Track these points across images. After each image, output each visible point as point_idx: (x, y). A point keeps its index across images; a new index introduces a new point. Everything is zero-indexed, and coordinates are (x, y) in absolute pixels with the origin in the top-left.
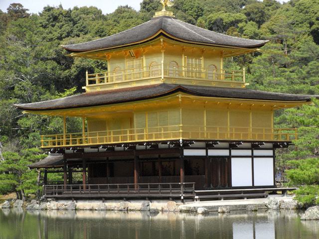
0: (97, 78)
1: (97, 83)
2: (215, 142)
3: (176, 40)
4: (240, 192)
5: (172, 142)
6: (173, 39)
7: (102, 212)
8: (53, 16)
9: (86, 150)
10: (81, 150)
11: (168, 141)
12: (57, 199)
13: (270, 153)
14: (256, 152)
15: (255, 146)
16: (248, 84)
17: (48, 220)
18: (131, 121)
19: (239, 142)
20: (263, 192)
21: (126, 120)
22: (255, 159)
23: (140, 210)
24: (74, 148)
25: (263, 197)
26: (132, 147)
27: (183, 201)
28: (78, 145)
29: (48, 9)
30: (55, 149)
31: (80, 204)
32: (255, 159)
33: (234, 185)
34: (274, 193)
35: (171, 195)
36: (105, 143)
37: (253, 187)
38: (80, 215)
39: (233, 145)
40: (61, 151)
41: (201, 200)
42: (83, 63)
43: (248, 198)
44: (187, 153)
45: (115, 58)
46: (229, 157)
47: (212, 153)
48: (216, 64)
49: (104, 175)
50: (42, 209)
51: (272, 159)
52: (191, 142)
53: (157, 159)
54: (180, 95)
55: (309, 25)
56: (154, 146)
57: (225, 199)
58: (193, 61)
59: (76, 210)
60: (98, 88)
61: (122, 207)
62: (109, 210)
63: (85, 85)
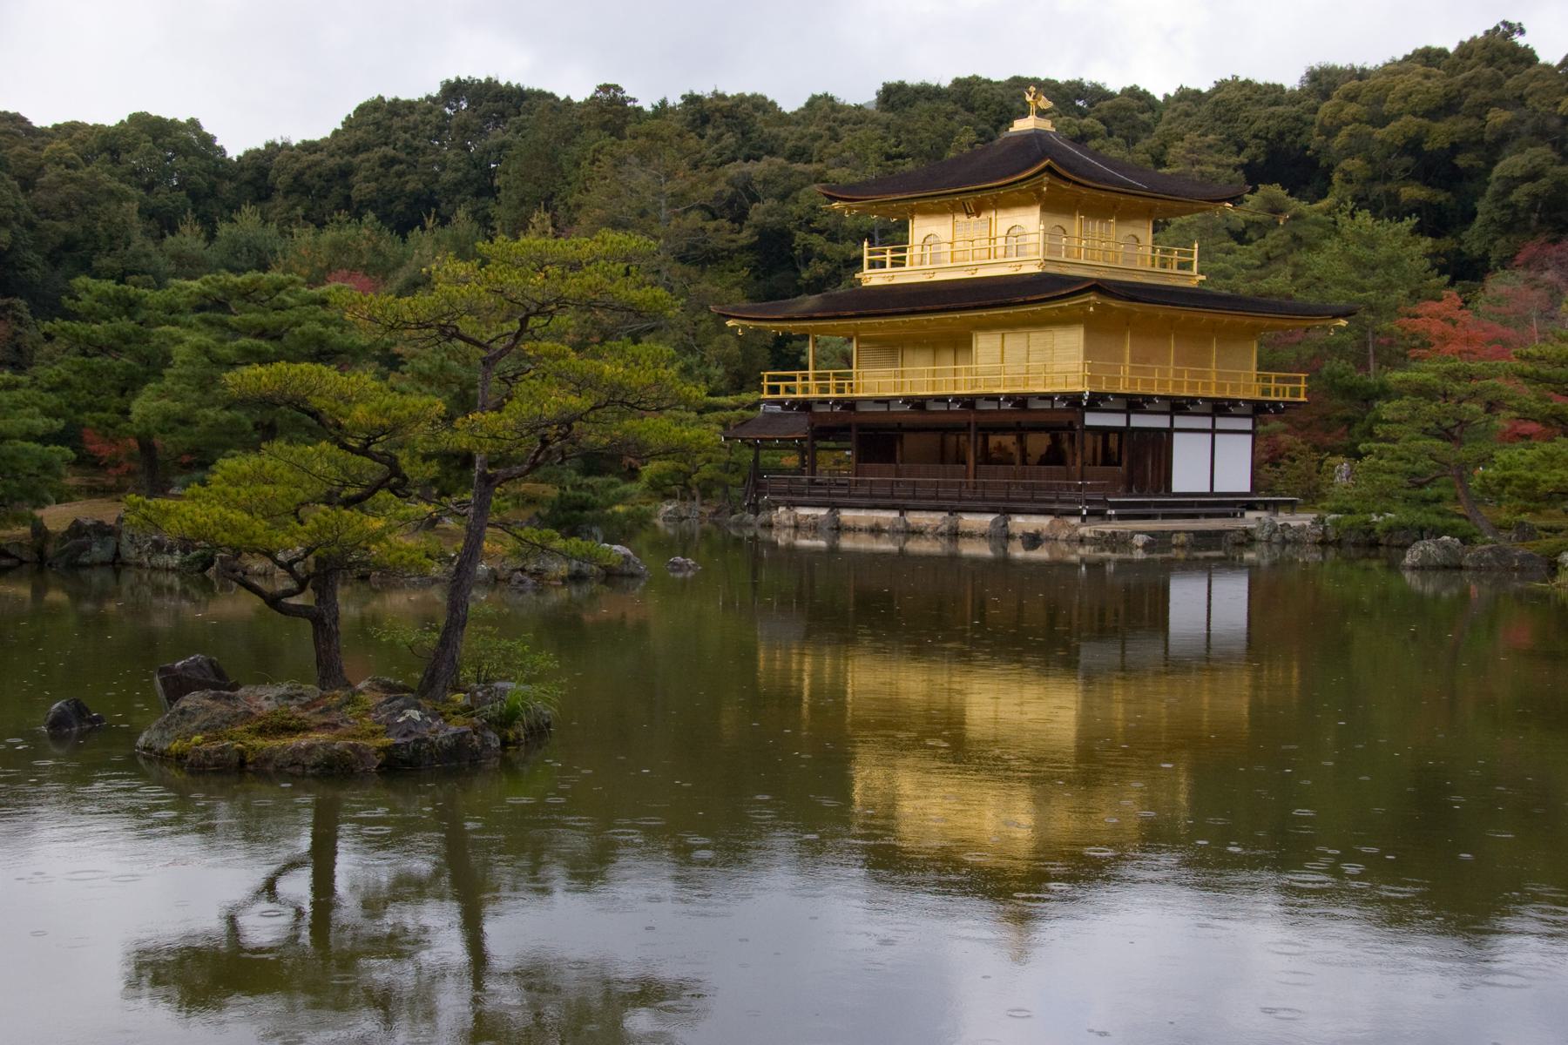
0: (888, 256)
1: (888, 268)
2: (1149, 398)
3: (1076, 183)
4: (1191, 504)
5: (1064, 397)
7: (901, 538)
8: (703, 114)
9: (861, 408)
10: (850, 405)
12: (791, 505)
13: (1247, 424)
14: (1222, 423)
15: (1220, 408)
16: (1203, 278)
17: (773, 545)
19: (1193, 400)
20: (1234, 504)
21: (960, 344)
22: (1217, 436)
23: (983, 536)
24: (837, 401)
25: (1235, 515)
26: (969, 402)
27: (1083, 520)
28: (847, 394)
29: (692, 100)
30: (794, 402)
31: (846, 515)
32: (1217, 436)
33: (1179, 485)
34: (1251, 506)
35: (1056, 506)
36: (907, 392)
37: (1212, 493)
38: (846, 543)
40: (805, 405)
41: (1120, 517)
42: (769, 219)
43: (1208, 516)
44: (1092, 419)
45: (927, 212)
46: (1170, 431)
47: (1138, 421)
48: (1140, 233)
49: (890, 458)
50: (763, 526)
51: (1249, 438)
52: (1103, 397)
54: (1093, 298)
55: (1235, 149)
56: (1020, 401)
57: (1165, 517)
58: (1096, 227)
59: (838, 529)
60: (902, 277)
61: (944, 528)
62: (914, 532)
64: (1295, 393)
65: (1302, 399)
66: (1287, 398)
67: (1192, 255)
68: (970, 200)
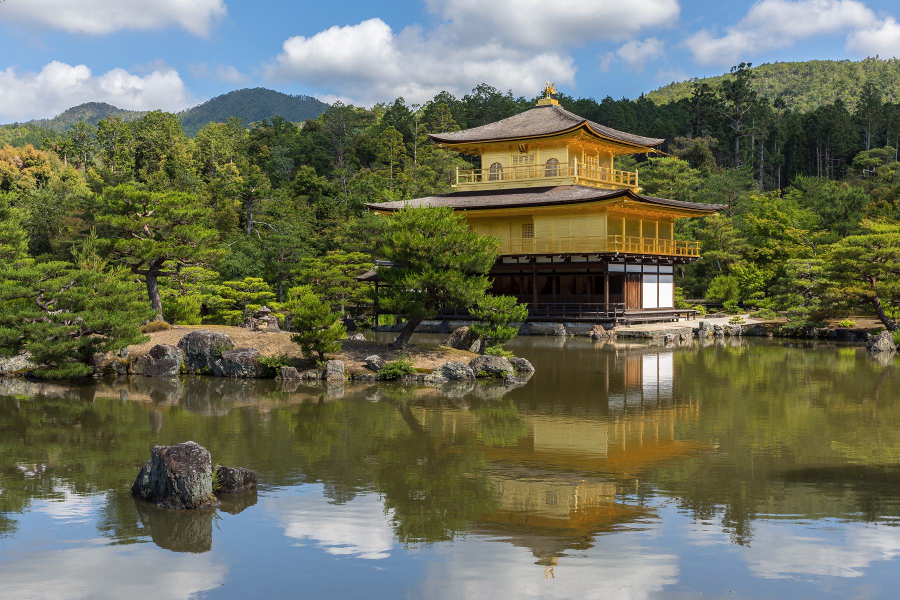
2: (639, 256)
4: (657, 315)
6: (591, 133)
11: (595, 254)
13: (670, 269)
14: (663, 269)
15: (662, 262)
18: (531, 226)
22: (660, 276)
26: (532, 258)
33: (645, 306)
37: (658, 309)
39: (647, 260)
46: (642, 274)
47: (631, 268)
51: (671, 277)
53: (551, 274)
56: (567, 257)
63: (454, 183)
64: (695, 254)
65: (698, 256)
66: (692, 255)
67: (634, 176)
68: (523, 144)
